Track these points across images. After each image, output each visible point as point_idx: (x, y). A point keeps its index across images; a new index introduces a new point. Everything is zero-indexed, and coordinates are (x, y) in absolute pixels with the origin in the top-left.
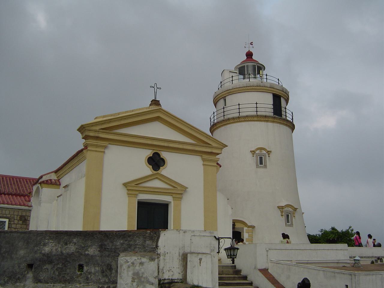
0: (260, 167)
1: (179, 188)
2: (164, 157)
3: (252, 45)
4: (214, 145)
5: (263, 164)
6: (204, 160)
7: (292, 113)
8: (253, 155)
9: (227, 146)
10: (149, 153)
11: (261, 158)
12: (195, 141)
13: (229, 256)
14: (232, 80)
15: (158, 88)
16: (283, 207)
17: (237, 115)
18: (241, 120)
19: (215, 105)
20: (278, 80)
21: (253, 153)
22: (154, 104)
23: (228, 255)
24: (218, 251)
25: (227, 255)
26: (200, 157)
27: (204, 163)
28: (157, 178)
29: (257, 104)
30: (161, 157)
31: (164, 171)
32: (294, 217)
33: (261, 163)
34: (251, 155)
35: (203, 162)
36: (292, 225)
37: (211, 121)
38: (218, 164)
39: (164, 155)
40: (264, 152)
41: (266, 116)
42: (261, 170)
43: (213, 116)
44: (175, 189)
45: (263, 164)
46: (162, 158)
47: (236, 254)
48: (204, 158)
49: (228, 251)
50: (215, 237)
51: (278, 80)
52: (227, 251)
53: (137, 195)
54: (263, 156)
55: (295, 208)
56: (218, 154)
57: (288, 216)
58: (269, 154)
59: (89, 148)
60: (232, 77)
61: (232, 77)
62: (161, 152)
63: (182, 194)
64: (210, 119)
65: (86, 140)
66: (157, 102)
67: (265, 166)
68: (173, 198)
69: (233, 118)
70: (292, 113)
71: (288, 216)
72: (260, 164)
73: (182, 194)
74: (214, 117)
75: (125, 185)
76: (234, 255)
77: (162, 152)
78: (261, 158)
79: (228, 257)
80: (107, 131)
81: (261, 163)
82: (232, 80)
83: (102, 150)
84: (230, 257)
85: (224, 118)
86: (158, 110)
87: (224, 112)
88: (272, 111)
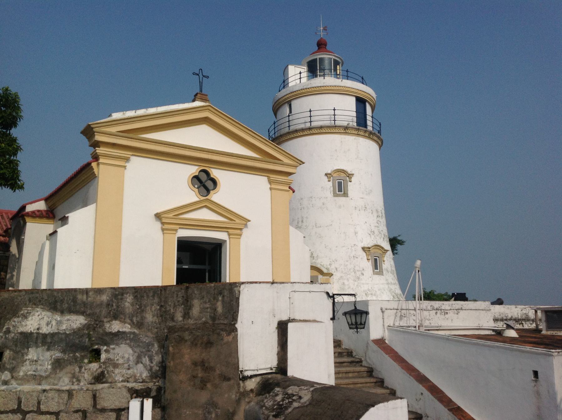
1: (238, 221)
2: (217, 178)
3: (326, 30)
4: (286, 161)
5: (342, 192)
6: (270, 182)
7: (380, 125)
8: (329, 180)
9: (304, 163)
10: (193, 170)
11: (340, 184)
12: (257, 154)
14: (300, 78)
15: (204, 76)
16: (369, 248)
17: (308, 125)
18: (313, 131)
19: (275, 114)
20: (362, 78)
21: (328, 176)
22: (200, 100)
23: (350, 323)
24: (331, 316)
25: (348, 323)
26: (266, 178)
27: (272, 187)
28: (206, 207)
29: (334, 110)
30: (212, 176)
31: (216, 197)
32: (384, 261)
33: (340, 190)
34: (326, 179)
35: (271, 185)
36: (381, 273)
37: (269, 134)
38: (290, 188)
39: (215, 173)
40: (343, 175)
42: (342, 200)
43: (273, 127)
44: (231, 222)
45: (342, 192)
46: (213, 178)
47: (365, 323)
48: (271, 178)
49: (351, 317)
50: (328, 293)
51: (362, 78)
52: (348, 316)
53: (176, 230)
54: (342, 181)
55: (385, 250)
56: (290, 174)
57: (376, 260)
58: (350, 178)
59: (101, 160)
60: (300, 73)
61: (300, 73)
62: (212, 169)
63: (241, 229)
64: (269, 131)
65: (97, 148)
66: (205, 96)
67: (346, 195)
68: (229, 235)
69: (303, 130)
70: (380, 125)
71: (376, 260)
73: (241, 229)
74: (274, 128)
75: (158, 216)
76: (361, 324)
77: (212, 170)
79: (351, 326)
80: (131, 135)
82: (300, 78)
83: (122, 163)
84: (354, 326)
85: (289, 130)
86: (207, 108)
87: (289, 121)
88: (355, 119)
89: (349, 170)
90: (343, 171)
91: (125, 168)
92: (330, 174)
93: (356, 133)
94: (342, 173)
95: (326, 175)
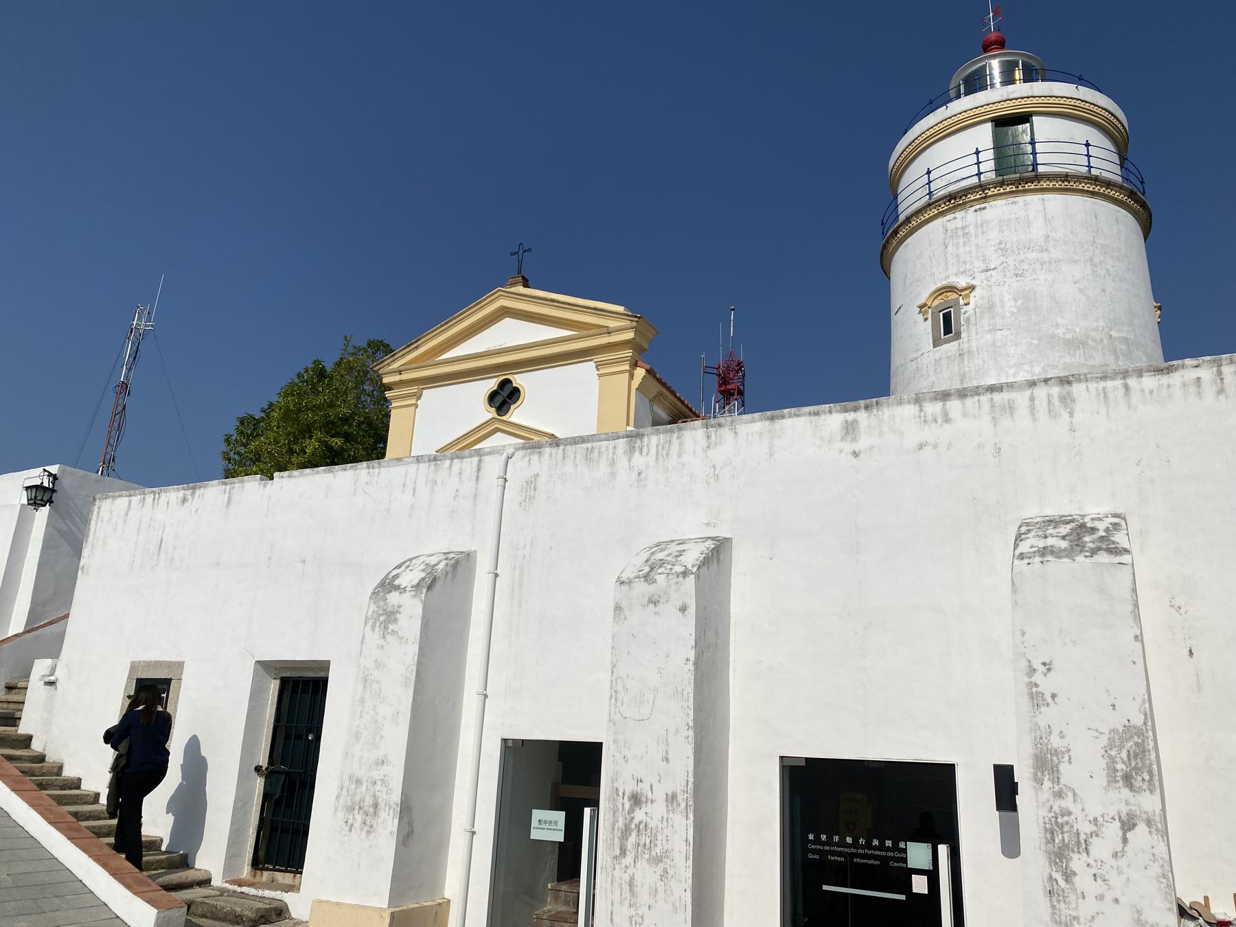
0: (948, 341)
10: (492, 384)
11: (947, 318)
13: (31, 499)
31: (517, 415)
33: (948, 330)
39: (519, 380)
40: (952, 296)
41: (951, 197)
59: (394, 405)
62: (515, 376)
67: (958, 336)
72: (944, 335)
78: (947, 318)
79: (31, 502)
81: (948, 330)
83: (413, 401)
89: (962, 282)
90: (951, 289)
91: (417, 407)
92: (924, 305)
93: (978, 196)
94: (949, 294)
95: (921, 307)
